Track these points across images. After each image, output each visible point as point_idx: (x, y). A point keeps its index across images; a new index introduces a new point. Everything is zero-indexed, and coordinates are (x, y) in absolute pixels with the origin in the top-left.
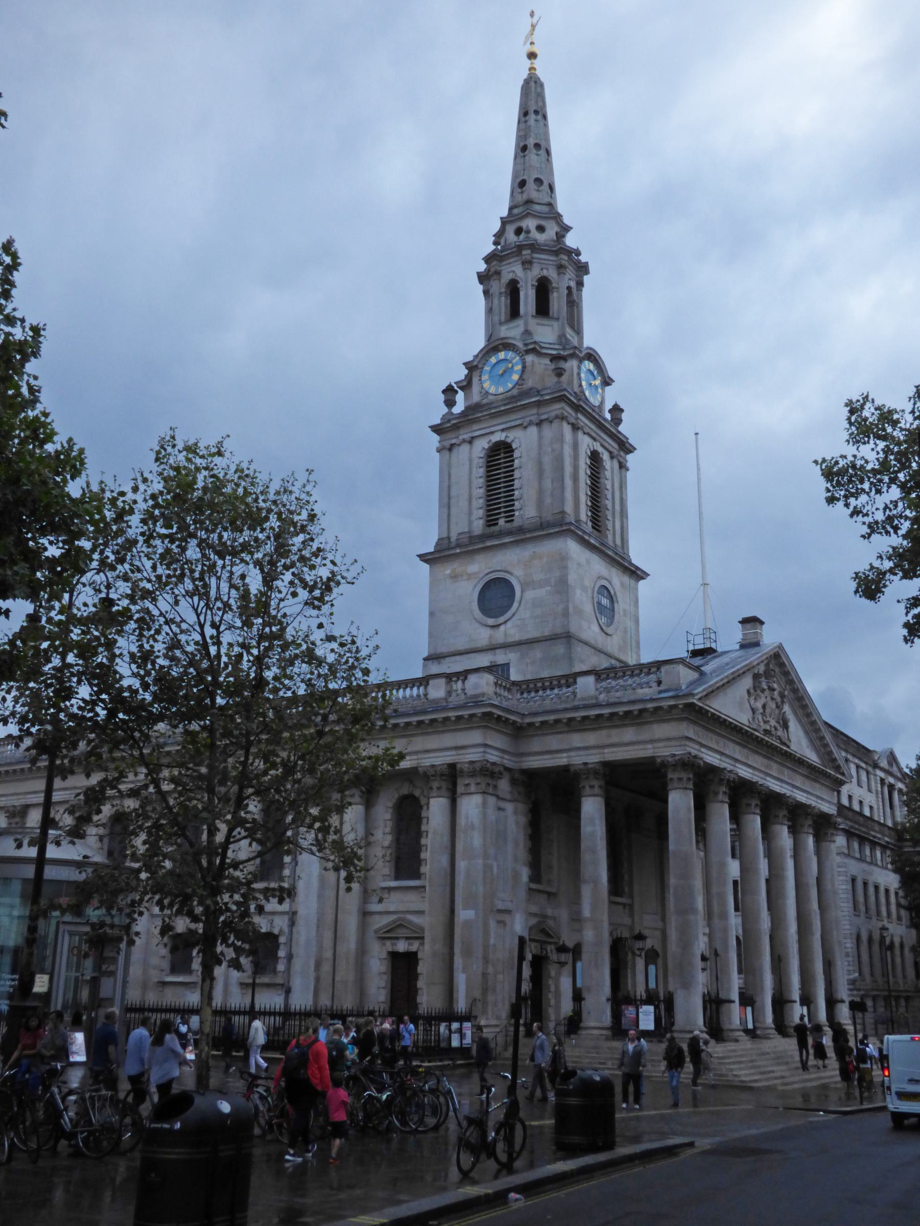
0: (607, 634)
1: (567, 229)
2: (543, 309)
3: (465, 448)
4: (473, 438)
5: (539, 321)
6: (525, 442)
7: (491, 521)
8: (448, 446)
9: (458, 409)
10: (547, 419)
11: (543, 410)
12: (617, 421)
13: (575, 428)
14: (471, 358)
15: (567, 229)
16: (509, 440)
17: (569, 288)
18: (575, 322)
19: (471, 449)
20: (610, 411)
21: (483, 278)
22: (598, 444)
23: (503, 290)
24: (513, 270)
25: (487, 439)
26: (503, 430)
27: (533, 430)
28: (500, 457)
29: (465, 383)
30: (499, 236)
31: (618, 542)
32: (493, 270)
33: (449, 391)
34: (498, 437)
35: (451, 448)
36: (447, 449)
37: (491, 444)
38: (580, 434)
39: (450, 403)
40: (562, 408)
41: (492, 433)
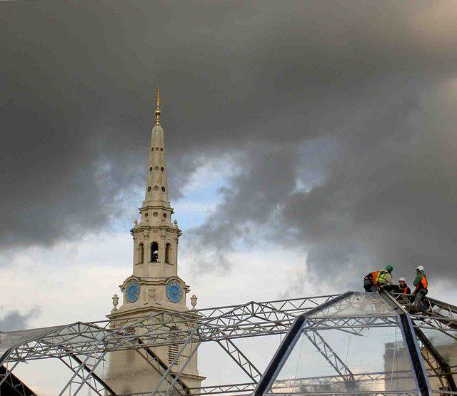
2: (154, 259)
12: (194, 305)
33: (116, 299)
39: (116, 304)
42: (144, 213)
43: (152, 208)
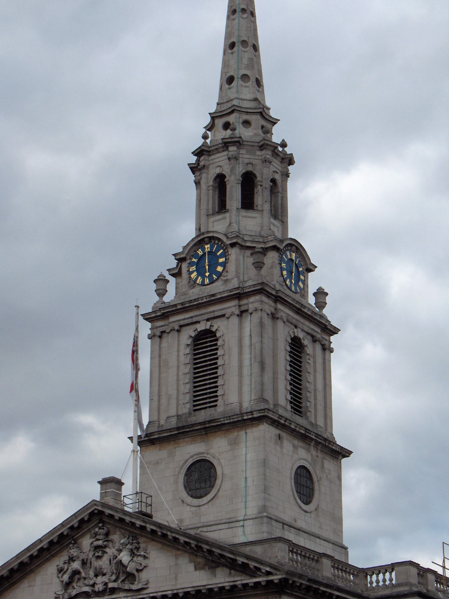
0: (306, 512)
1: (274, 122)
2: (248, 203)
4: (181, 326)
5: (244, 213)
6: (227, 330)
7: (197, 407)
8: (158, 333)
9: (170, 297)
10: (247, 311)
11: (244, 302)
12: (321, 305)
13: (274, 317)
14: (181, 250)
15: (274, 122)
16: (214, 329)
17: (273, 181)
18: (279, 212)
19: (179, 336)
20: (315, 294)
21: (194, 168)
22: (299, 330)
23: (211, 183)
24: (219, 163)
25: (193, 327)
26: (208, 320)
27: (235, 320)
28: (205, 344)
29: (176, 271)
30: (210, 127)
31: (321, 422)
32: (202, 163)
33: (161, 281)
35: (160, 337)
36: (157, 336)
38: (280, 323)
39: (161, 293)
40: (262, 301)
41: (198, 322)
42: (220, 123)
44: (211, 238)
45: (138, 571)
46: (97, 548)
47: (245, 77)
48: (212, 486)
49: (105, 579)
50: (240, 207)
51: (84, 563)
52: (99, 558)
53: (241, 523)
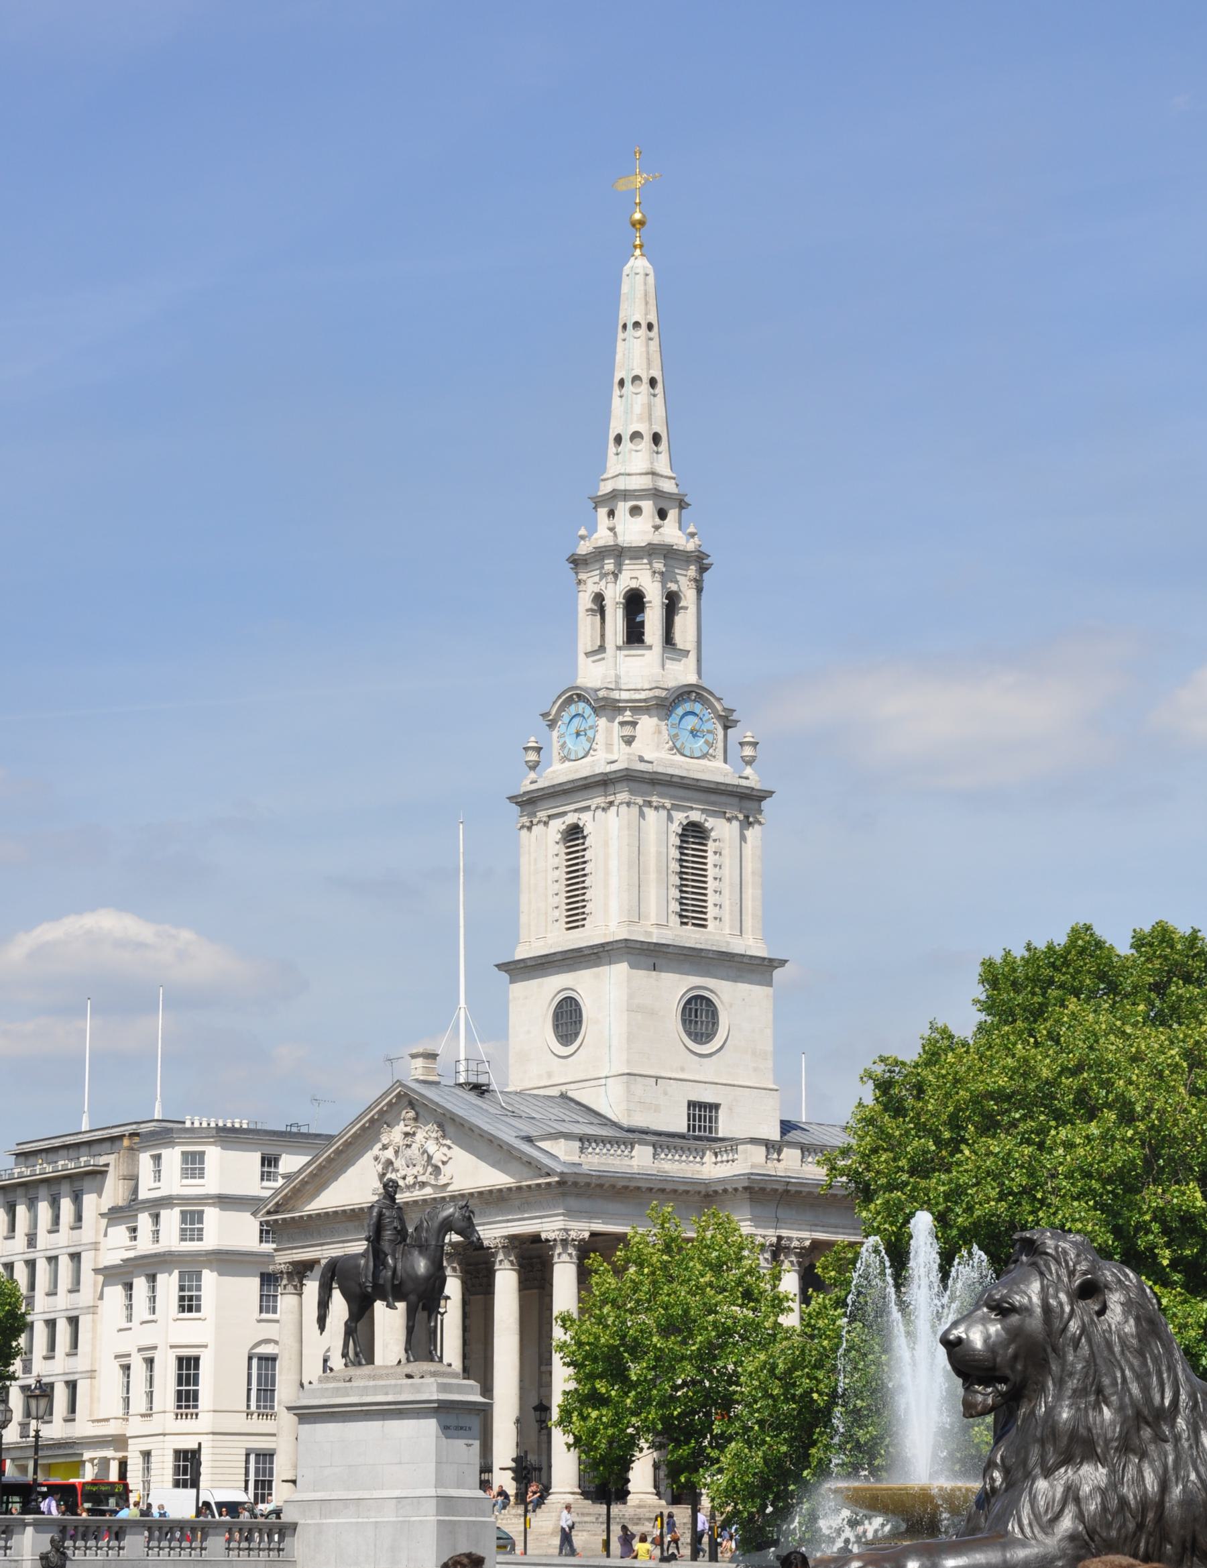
2: (635, 635)
3: (541, 826)
4: (549, 816)
25: (561, 820)
26: (576, 811)
34: (571, 819)
37: (564, 827)
41: (565, 813)
43: (625, 495)
44: (579, 695)
45: (444, 1163)
46: (407, 1134)
47: (636, 435)
48: (577, 1034)
49: (415, 1171)
50: (620, 642)
51: (396, 1152)
52: (409, 1146)
53: (603, 1081)
